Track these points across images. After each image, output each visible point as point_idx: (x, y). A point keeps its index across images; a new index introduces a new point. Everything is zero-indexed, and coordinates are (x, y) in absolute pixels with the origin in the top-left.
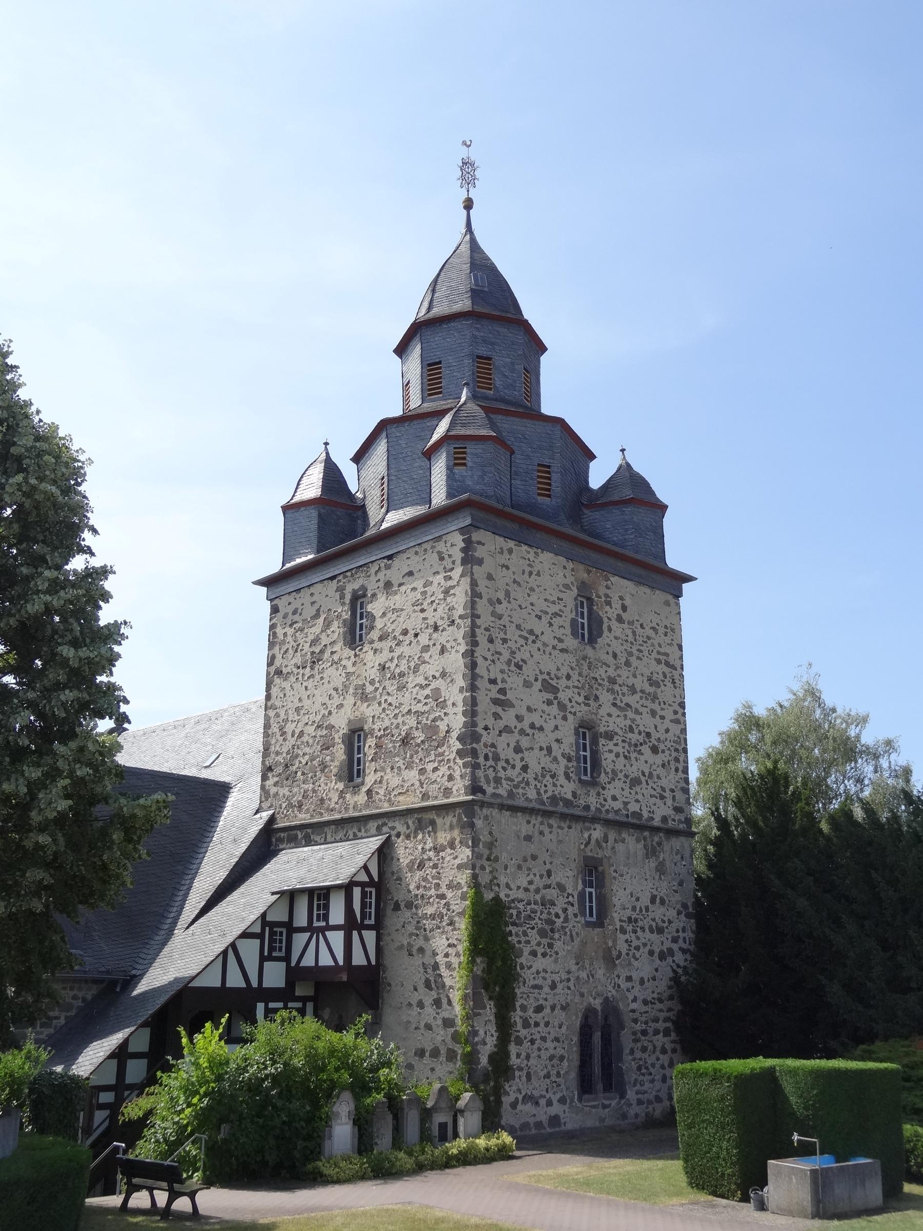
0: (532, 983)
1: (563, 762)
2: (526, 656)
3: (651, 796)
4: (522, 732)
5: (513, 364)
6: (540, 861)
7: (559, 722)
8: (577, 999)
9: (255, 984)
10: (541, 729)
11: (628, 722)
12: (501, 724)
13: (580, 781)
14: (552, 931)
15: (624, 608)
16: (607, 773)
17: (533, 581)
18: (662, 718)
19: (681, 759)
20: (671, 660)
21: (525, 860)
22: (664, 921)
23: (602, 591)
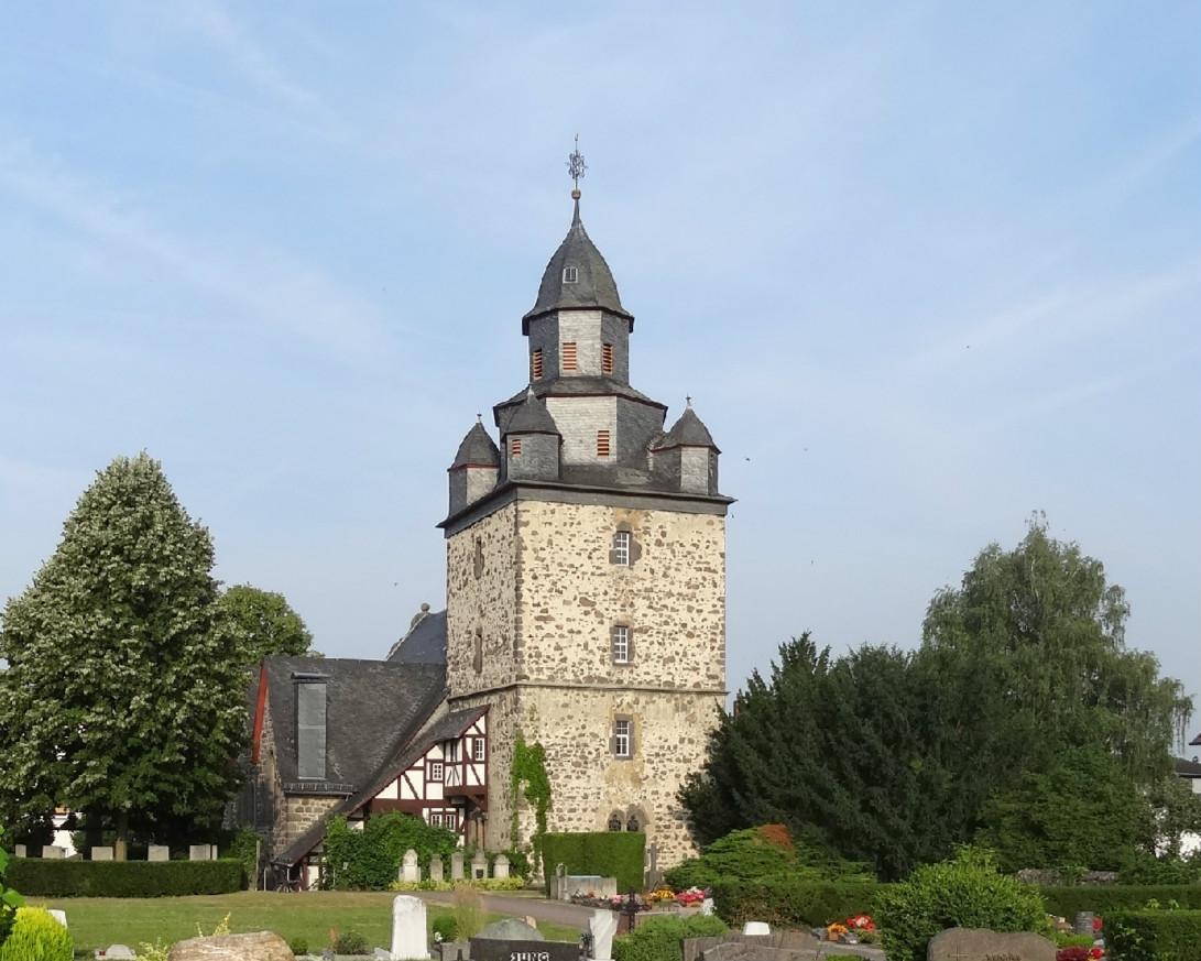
0: (567, 795)
1: (599, 654)
2: (567, 584)
3: (684, 669)
4: (562, 636)
5: (593, 345)
6: (575, 719)
7: (596, 625)
8: (607, 805)
9: (421, 797)
10: (579, 632)
11: (664, 619)
12: (543, 633)
13: (614, 664)
14: (586, 763)
15: (664, 534)
16: (640, 657)
17: (573, 530)
18: (700, 611)
19: (718, 639)
20: (713, 567)
21: (563, 719)
22: (691, 755)
23: (641, 524)
